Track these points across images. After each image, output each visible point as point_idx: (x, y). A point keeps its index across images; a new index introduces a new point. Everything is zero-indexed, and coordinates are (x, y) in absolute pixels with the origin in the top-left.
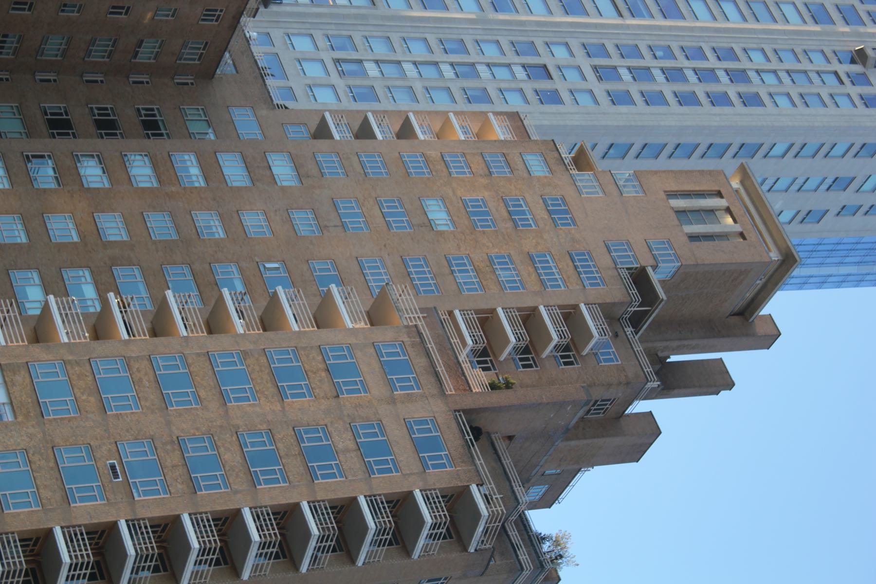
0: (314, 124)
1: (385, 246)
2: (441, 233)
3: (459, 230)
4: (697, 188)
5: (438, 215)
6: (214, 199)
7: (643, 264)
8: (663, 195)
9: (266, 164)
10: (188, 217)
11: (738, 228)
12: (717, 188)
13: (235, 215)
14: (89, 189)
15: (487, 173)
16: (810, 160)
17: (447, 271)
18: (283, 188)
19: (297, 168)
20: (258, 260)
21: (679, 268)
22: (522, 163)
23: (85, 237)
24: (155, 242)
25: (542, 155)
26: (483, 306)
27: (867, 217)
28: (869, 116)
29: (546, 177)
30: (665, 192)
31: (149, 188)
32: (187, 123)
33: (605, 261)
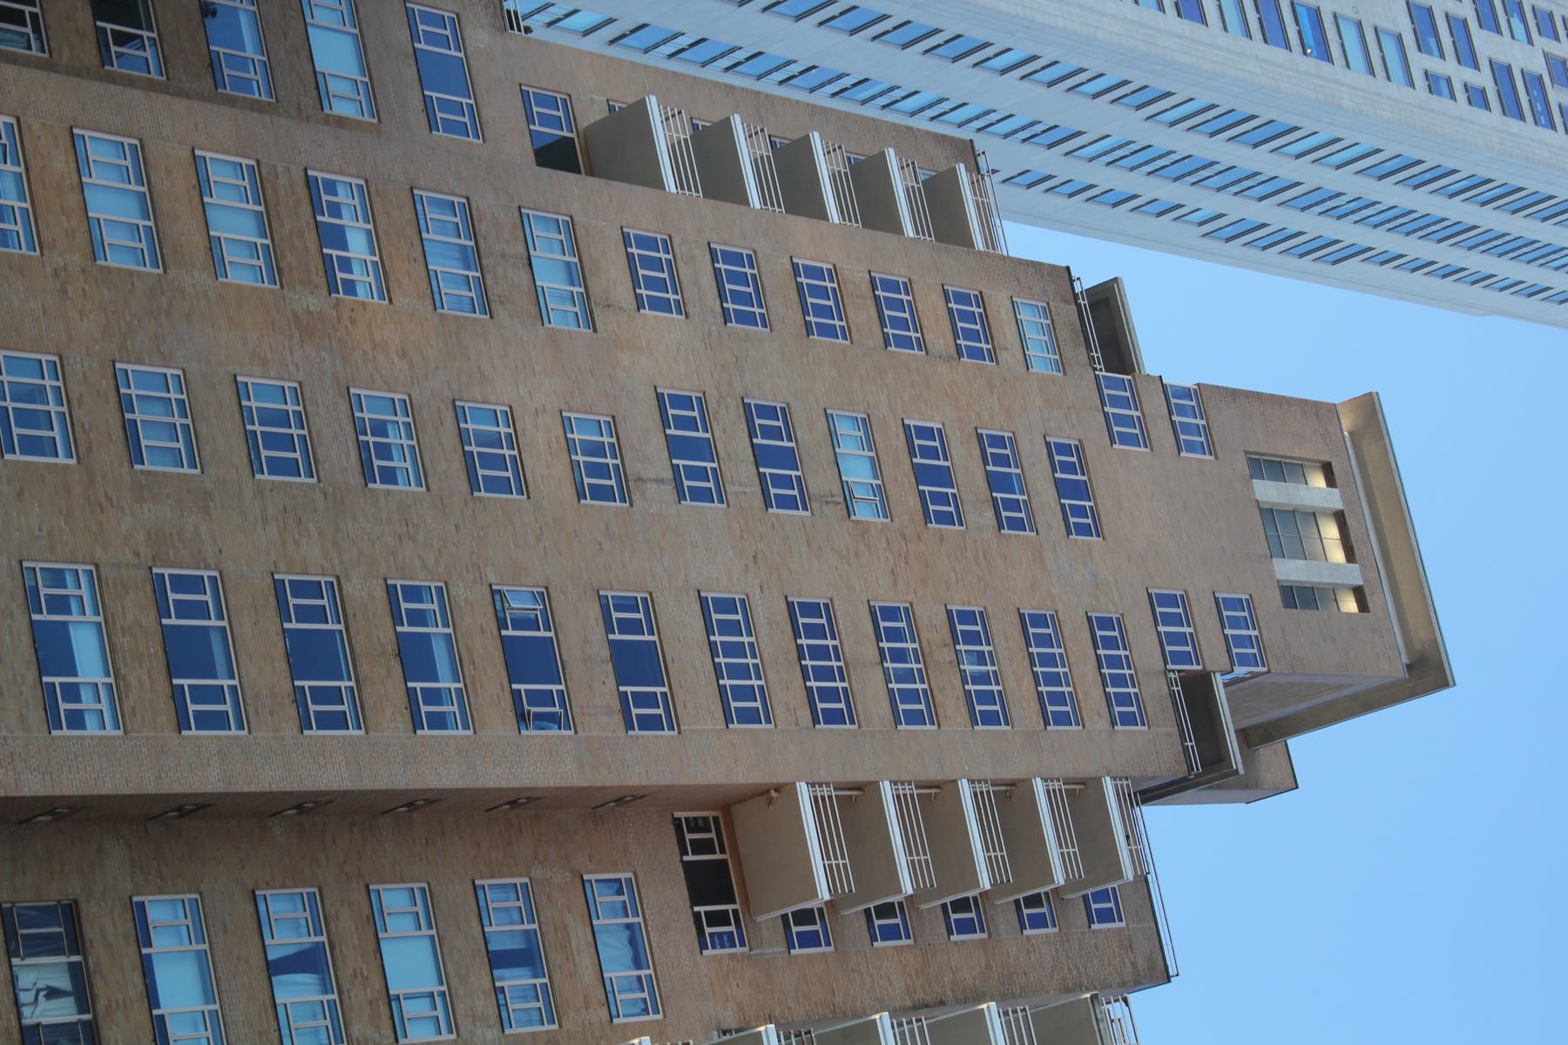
0: (591, 113)
1: (755, 557)
2: (864, 528)
3: (897, 524)
4: (1297, 453)
5: (858, 473)
6: (404, 355)
7: (1209, 668)
8: (1243, 467)
9: (521, 249)
10: (343, 406)
11: (1354, 575)
12: (1326, 458)
13: (449, 415)
14: (107, 271)
15: (953, 351)
16: (1043, 88)
17: (873, 654)
18: (554, 338)
19: (578, 273)
20: (492, 579)
21: (1255, 675)
22: (1014, 328)
23: (89, 449)
24: (260, 490)
25: (1048, 312)
26: (934, 774)
27: (1048, 196)
28: (1180, 37)
29: (1053, 380)
30: (1246, 453)
31: (254, 289)
32: (310, 29)
33: (1144, 648)
